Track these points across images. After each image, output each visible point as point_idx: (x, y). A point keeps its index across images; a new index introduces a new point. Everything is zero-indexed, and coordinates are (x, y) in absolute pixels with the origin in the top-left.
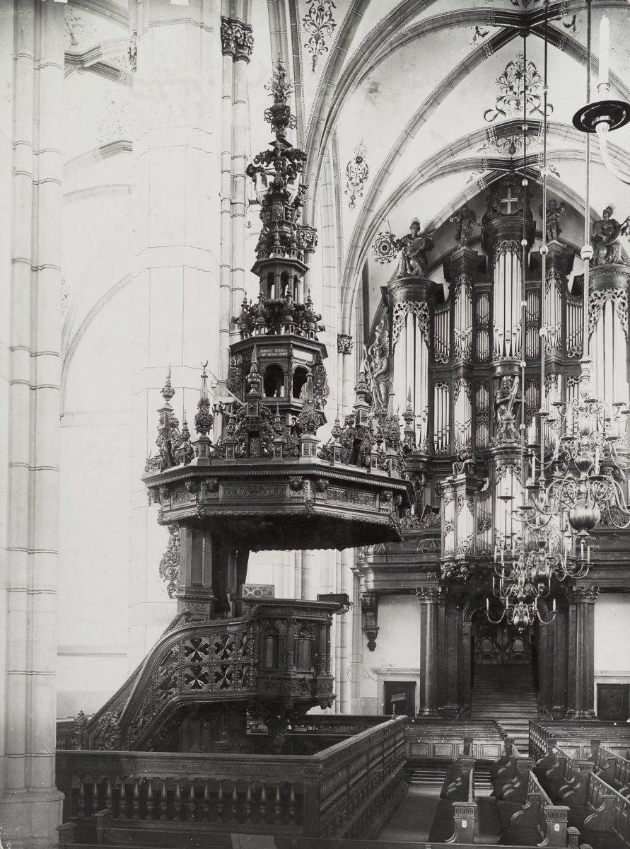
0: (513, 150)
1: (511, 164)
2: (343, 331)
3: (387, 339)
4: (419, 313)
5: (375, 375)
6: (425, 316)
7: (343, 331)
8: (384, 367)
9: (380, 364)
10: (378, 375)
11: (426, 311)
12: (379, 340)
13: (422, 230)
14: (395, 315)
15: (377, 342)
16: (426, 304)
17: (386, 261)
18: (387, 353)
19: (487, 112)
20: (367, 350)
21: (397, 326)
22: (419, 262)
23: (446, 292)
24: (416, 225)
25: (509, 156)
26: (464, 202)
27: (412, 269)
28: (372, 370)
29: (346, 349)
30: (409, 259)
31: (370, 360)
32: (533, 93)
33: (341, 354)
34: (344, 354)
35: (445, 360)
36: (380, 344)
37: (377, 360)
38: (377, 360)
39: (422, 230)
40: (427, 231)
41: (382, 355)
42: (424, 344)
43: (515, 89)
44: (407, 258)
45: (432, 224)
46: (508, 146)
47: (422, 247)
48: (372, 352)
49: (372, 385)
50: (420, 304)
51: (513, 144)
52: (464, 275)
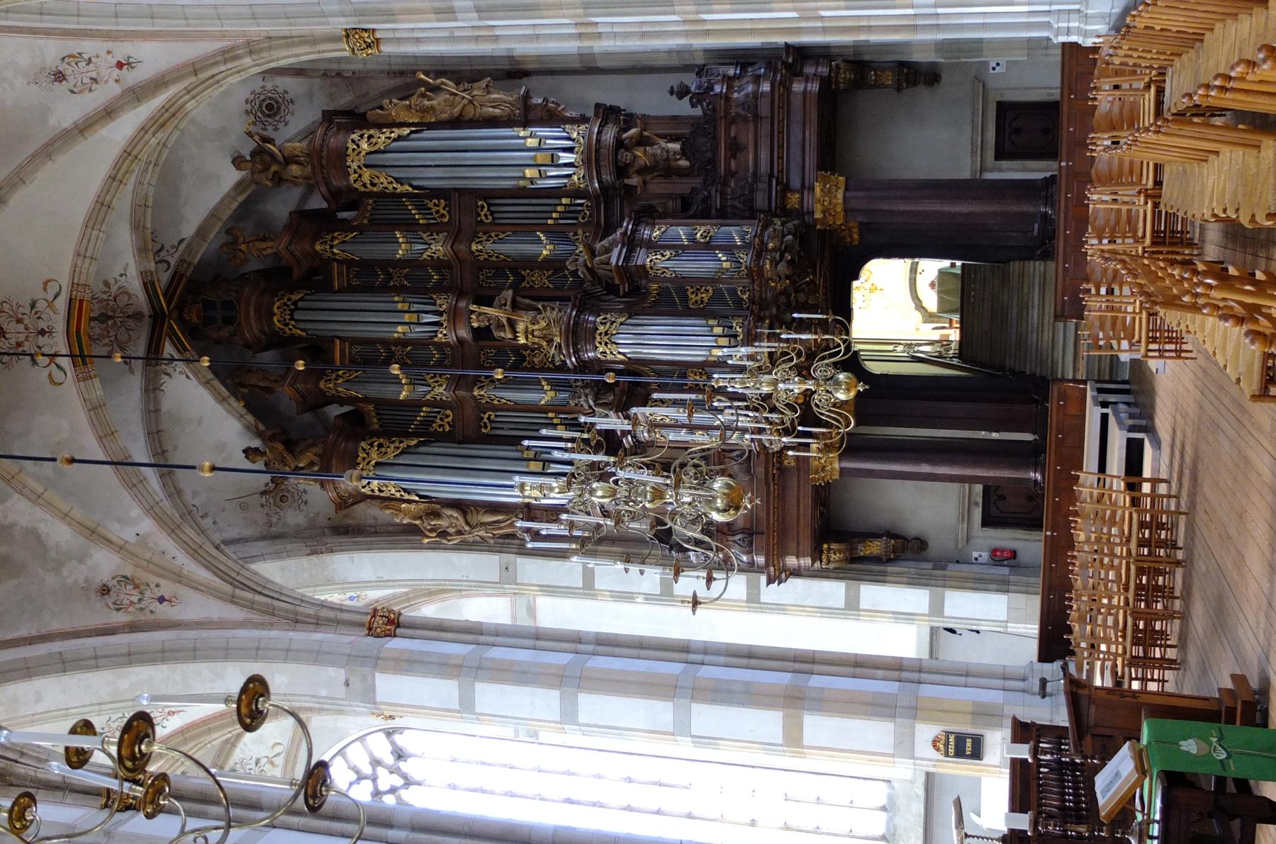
0: (138, 316)
1: (158, 318)
2: (361, 625)
3: (413, 506)
4: (375, 457)
5: (467, 528)
6: (380, 446)
7: (361, 625)
8: (456, 515)
9: (450, 519)
10: (468, 524)
11: (371, 445)
12: (415, 518)
13: (256, 443)
14: (377, 493)
15: (417, 522)
16: (363, 444)
17: (305, 497)
18: (435, 507)
19: (52, 382)
20: (428, 537)
21: (393, 491)
22: (303, 452)
23: (346, 409)
24: (249, 453)
25: (147, 319)
26: (216, 383)
27: (312, 464)
28: (460, 533)
29: (390, 622)
30: (297, 467)
31: (443, 534)
32: (28, 311)
33: (399, 631)
34: (398, 626)
35: (448, 416)
36: (420, 518)
37: (443, 523)
38: (443, 523)
39: (256, 443)
40: (259, 434)
41: (437, 515)
42: (422, 449)
43: (22, 338)
44: (297, 471)
45: (247, 427)
46: (131, 323)
47: (280, 447)
48: (431, 531)
49: (482, 533)
50: (362, 455)
51: (129, 317)
52: (322, 385)
